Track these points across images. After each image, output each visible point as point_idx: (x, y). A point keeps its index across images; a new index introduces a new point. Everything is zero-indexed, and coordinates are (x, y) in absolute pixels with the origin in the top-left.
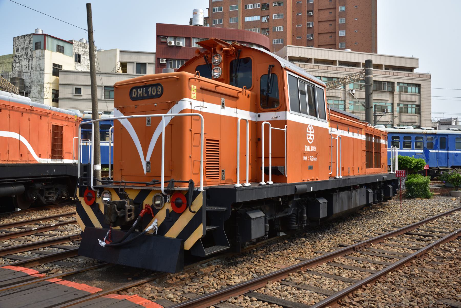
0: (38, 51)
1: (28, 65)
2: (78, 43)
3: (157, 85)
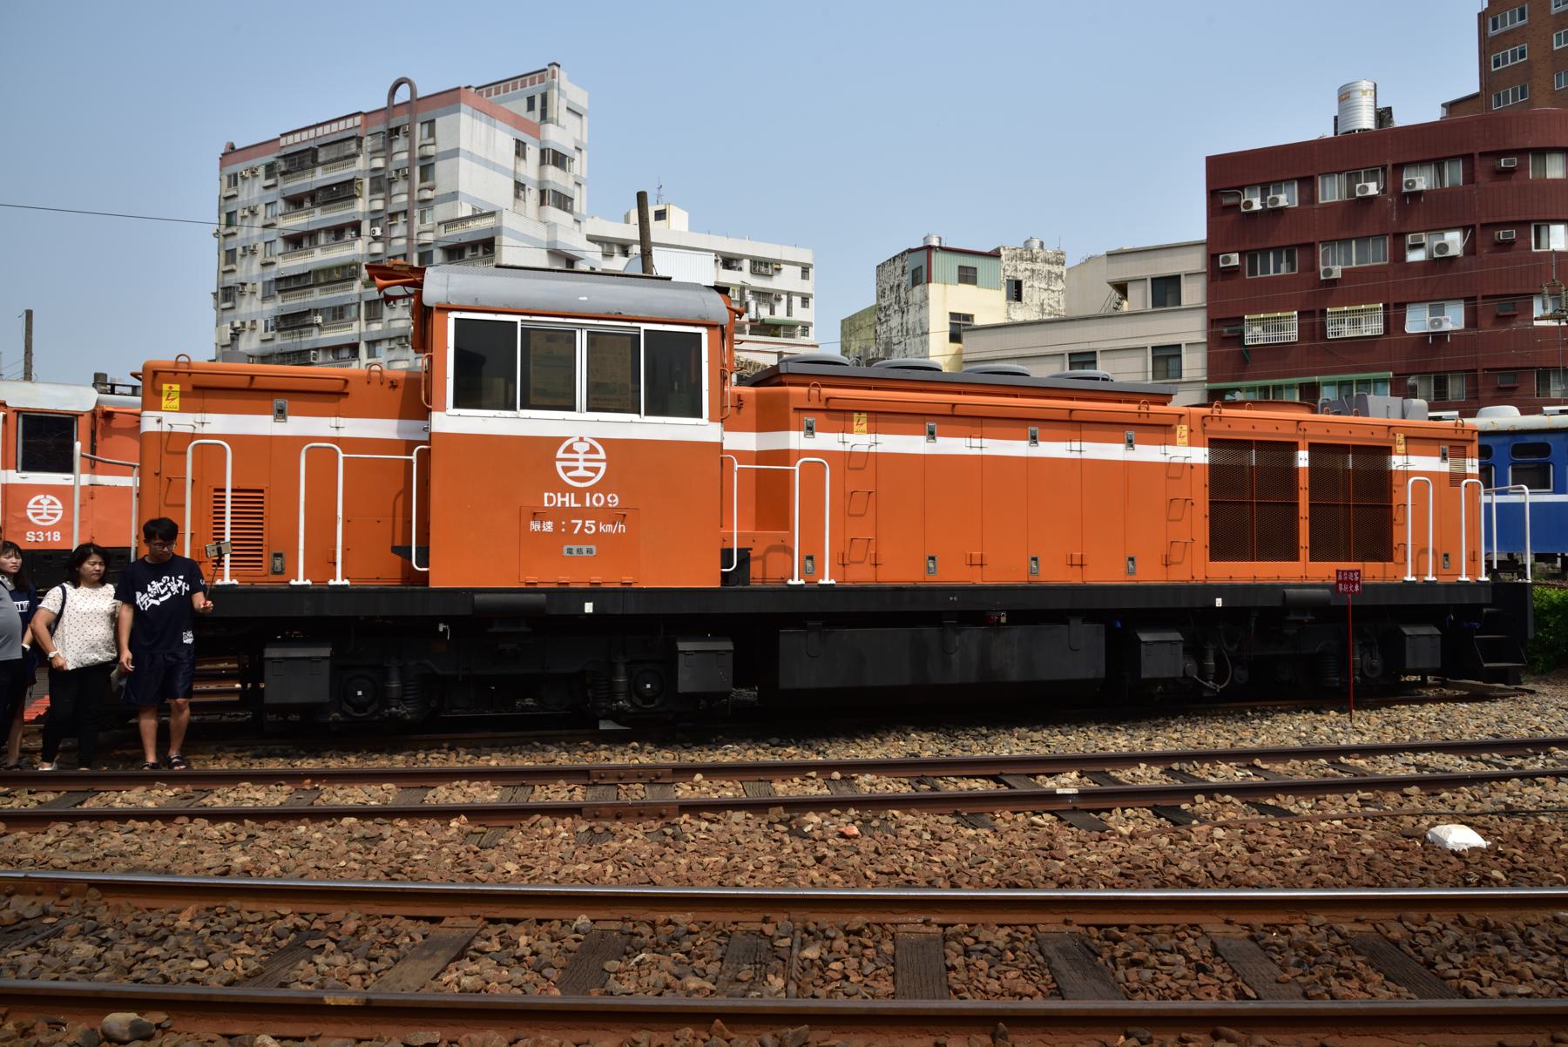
0: (918, 288)
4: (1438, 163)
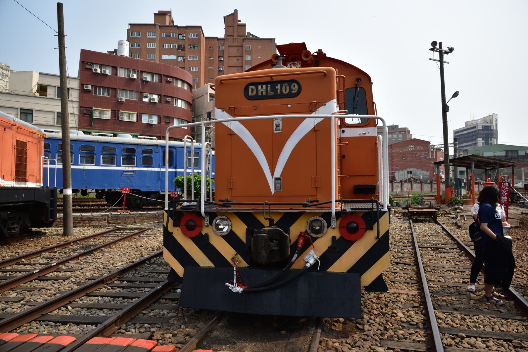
3: (290, 82)
4: (152, 74)
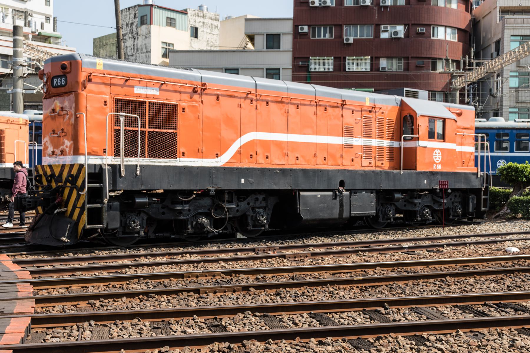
0: (144, 27)
1: (134, 45)
2: (194, 12)
